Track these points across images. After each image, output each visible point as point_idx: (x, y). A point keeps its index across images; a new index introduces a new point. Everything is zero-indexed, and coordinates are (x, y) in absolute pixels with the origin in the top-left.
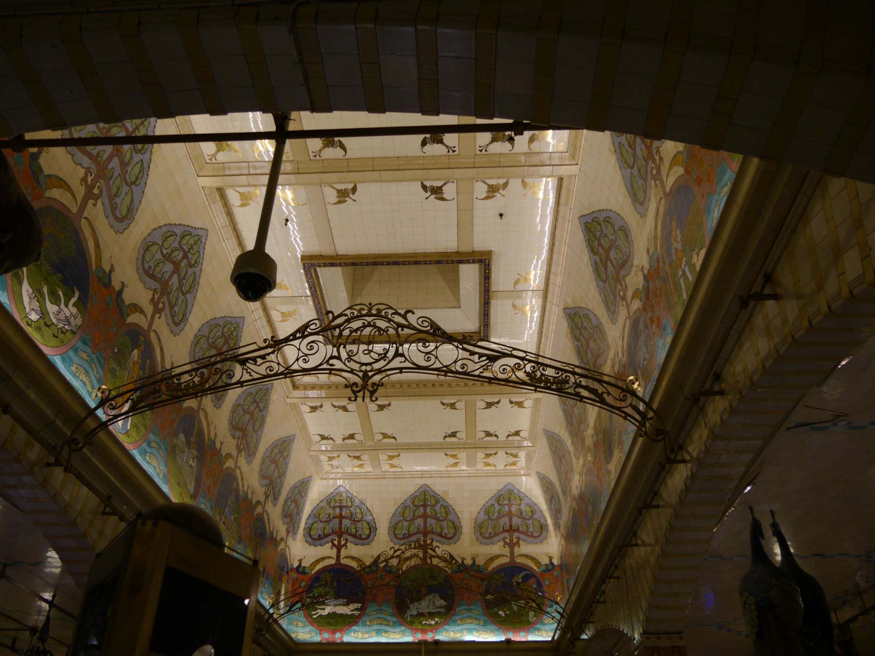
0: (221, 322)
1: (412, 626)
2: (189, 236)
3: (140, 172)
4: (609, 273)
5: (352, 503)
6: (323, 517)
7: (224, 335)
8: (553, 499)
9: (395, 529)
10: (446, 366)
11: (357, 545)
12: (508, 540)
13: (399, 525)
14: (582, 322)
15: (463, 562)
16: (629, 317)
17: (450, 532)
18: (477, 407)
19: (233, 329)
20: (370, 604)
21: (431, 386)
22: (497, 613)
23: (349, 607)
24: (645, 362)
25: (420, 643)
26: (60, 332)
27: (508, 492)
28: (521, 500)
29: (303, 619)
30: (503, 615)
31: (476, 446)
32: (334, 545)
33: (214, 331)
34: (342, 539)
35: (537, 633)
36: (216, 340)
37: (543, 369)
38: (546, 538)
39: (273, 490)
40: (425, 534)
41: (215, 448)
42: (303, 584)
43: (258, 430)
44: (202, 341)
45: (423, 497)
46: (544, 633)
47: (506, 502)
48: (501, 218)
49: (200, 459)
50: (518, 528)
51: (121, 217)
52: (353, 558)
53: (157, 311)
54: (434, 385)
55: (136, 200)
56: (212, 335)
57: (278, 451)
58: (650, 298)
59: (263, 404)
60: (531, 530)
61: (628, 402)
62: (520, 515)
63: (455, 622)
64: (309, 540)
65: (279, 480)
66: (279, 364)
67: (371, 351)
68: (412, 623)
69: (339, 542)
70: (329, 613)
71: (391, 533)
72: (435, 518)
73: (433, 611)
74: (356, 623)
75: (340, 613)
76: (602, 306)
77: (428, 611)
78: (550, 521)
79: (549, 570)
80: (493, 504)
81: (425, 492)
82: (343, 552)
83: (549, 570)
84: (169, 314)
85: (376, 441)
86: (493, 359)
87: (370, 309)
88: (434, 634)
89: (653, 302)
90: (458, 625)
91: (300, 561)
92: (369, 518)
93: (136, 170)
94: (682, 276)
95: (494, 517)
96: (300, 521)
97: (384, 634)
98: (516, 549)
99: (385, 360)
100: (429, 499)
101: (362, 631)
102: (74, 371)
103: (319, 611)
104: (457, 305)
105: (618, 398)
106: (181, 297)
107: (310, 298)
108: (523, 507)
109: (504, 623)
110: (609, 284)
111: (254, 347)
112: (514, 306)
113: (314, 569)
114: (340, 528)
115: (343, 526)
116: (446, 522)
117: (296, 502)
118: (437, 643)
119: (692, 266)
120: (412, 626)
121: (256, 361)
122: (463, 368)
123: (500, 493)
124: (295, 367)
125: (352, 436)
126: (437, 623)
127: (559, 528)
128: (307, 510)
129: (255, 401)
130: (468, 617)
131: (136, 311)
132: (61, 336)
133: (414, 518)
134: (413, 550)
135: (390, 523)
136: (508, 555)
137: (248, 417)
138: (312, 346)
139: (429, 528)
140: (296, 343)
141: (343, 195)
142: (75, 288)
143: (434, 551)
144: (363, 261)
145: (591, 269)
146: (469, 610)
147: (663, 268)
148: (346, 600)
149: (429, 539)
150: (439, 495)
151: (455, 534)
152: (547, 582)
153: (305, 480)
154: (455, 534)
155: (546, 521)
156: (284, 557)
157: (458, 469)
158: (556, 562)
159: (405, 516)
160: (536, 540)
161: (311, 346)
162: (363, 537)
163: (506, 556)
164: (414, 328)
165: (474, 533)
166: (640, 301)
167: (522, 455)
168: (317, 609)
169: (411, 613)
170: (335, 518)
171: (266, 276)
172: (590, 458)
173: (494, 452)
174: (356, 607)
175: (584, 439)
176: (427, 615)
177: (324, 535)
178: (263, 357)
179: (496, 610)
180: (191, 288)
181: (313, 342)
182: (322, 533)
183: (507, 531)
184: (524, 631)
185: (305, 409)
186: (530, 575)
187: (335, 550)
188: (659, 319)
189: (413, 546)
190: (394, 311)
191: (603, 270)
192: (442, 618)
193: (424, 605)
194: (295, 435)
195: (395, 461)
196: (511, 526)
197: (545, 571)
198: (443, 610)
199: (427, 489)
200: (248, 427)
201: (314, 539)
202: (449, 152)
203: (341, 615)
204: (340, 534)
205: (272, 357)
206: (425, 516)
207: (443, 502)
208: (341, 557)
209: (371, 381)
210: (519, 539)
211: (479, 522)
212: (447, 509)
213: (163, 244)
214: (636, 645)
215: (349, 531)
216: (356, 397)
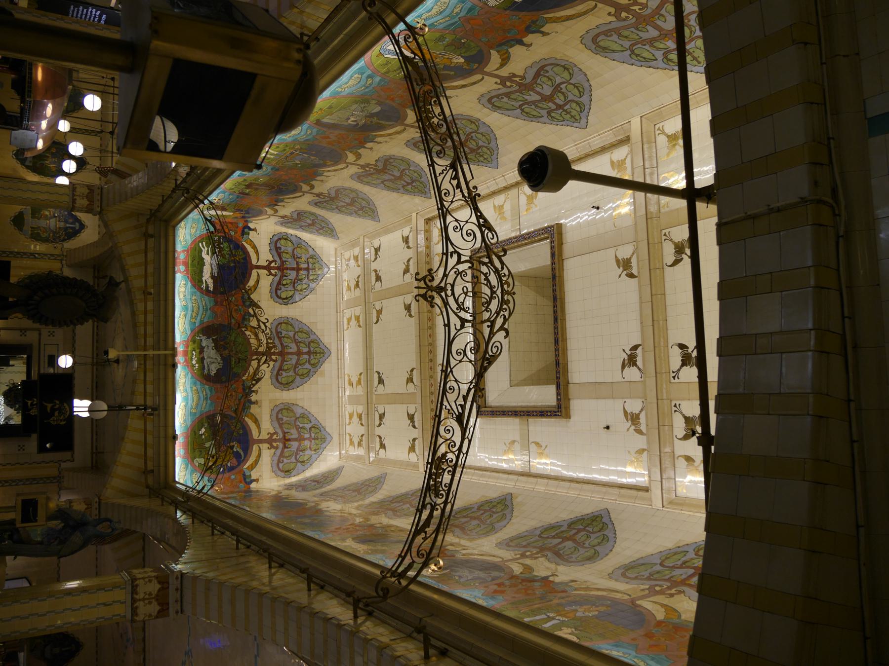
0: (493, 144)
2: (579, 110)
3: (645, 58)
4: (549, 540)
6: (298, 252)
7: (479, 148)
9: (286, 323)
10: (451, 371)
12: (275, 437)
14: (499, 512)
15: (254, 391)
16: (504, 561)
19: (485, 157)
20: (213, 299)
22: (202, 426)
24: (457, 578)
25: (174, 349)
27: (323, 437)
28: (315, 450)
29: (198, 233)
32: (271, 262)
33: (484, 138)
35: (183, 466)
36: (474, 140)
37: (449, 471)
38: (277, 476)
39: (324, 202)
40: (282, 354)
41: (366, 142)
42: (233, 233)
43: (385, 185)
44: (473, 126)
45: (318, 351)
46: (183, 474)
47: (313, 435)
48: (605, 428)
49: (356, 128)
50: (288, 448)
51: (597, 41)
52: (258, 282)
53: (503, 81)
54: (431, 360)
55: (616, 55)
56: (479, 136)
58: (524, 584)
59: (410, 189)
60: (285, 461)
61: (417, 559)
62: (300, 450)
63: (195, 384)
64: (276, 238)
65: (335, 207)
66: (452, 202)
67: (466, 295)
68: (194, 341)
69: (274, 268)
72: (297, 362)
73: (205, 362)
74: (194, 285)
76: (514, 534)
78: (294, 479)
79: (245, 479)
80: (311, 422)
83: (245, 479)
84: (500, 92)
86: (459, 419)
87: (509, 293)
89: (520, 586)
90: (191, 388)
91: (255, 230)
92: (297, 297)
93: (646, 54)
94: (548, 616)
95: (298, 423)
97: (183, 313)
98: (266, 445)
99: (457, 309)
103: (206, 249)
104: (513, 383)
105: (420, 549)
106: (517, 104)
107: (518, 233)
108: (308, 452)
109: (193, 432)
110: (538, 541)
111: (469, 177)
112: (514, 442)
114: (287, 269)
115: (289, 271)
117: (313, 224)
118: (174, 366)
119: (559, 627)
121: (454, 179)
122: (450, 388)
123: (322, 429)
124: (449, 219)
125: (378, 279)
126: (193, 366)
127: (288, 489)
128: (305, 236)
129: (413, 182)
130: (199, 398)
131: (503, 60)
133: (297, 343)
134: (265, 342)
135: (293, 319)
136: (260, 438)
137: (397, 174)
138: (471, 235)
139: (287, 357)
140: (474, 219)
141: (625, 264)
143: (265, 363)
144: (557, 286)
145: (552, 522)
146: (206, 399)
147: (555, 597)
148: (216, 275)
149: (276, 358)
151: (281, 383)
152: (233, 477)
154: (281, 383)
155: (294, 476)
156: (259, 213)
158: (253, 486)
159: (300, 334)
160: (275, 468)
161: (470, 234)
162: (279, 292)
163: (259, 435)
164: (490, 338)
166: (521, 573)
167: (361, 452)
168: (208, 247)
169: (203, 340)
170: (297, 263)
171: (545, 182)
172: (358, 520)
173: (363, 422)
176: (201, 356)
178: (459, 186)
179: (206, 425)
180: (527, 113)
181: (475, 236)
182: (282, 250)
183: (284, 436)
184: (185, 454)
185: (406, 232)
186: (240, 459)
187: (266, 264)
188: (503, 592)
189: (269, 341)
190: (507, 317)
191: (553, 534)
192: (198, 371)
193: (211, 353)
195: (354, 322)
196: (289, 440)
197: (244, 475)
198: (206, 372)
199: (326, 356)
201: (276, 244)
202: (673, 372)
203: (202, 271)
204: (281, 268)
205: (459, 196)
206: (299, 353)
208: (259, 271)
209: (434, 294)
210: (277, 448)
211: (294, 408)
212: (306, 375)
213: (571, 84)
214: (171, 566)
215: (284, 278)
216: (420, 280)
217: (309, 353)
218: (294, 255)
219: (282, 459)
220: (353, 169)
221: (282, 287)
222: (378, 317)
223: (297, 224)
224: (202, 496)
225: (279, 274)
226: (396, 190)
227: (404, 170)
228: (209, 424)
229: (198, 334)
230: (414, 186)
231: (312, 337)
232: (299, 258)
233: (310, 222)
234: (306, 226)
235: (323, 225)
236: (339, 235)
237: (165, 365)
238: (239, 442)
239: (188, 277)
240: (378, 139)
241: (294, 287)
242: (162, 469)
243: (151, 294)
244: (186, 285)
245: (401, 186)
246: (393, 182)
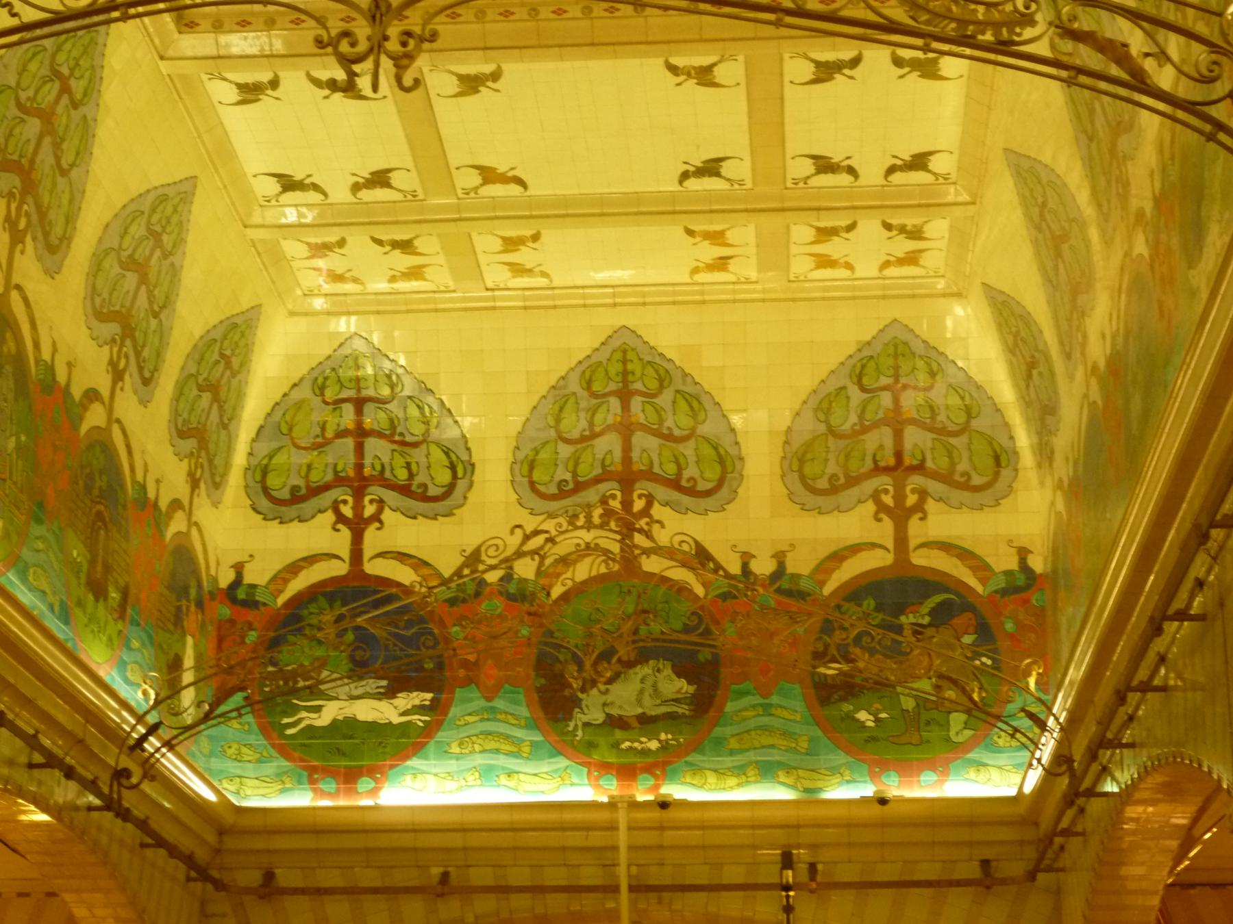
1: (589, 756)
6: (304, 433)
8: (1035, 372)
9: (531, 467)
11: (415, 518)
12: (888, 500)
13: (544, 455)
17: (708, 475)
18: (787, 79)
22: (850, 718)
23: (395, 702)
27: (891, 350)
28: (933, 374)
29: (258, 740)
30: (871, 724)
31: (788, 204)
32: (341, 518)
34: (367, 499)
39: (138, 354)
40: (627, 479)
42: (252, 636)
43: (72, 165)
45: (620, 367)
47: (884, 381)
50: (923, 461)
52: (402, 557)
57: (143, 232)
59: (83, 83)
60: (963, 466)
63: (719, 742)
64: (264, 503)
65: (154, 323)
68: (591, 745)
69: (358, 507)
70: (335, 721)
71: (518, 478)
72: (657, 434)
74: (416, 748)
75: (370, 719)
77: (640, 711)
78: (1023, 440)
80: (844, 388)
81: (625, 352)
82: (373, 540)
83: (1017, 590)
85: (460, 192)
88: (656, 777)
90: (732, 753)
91: (239, 568)
95: (847, 427)
96: (230, 448)
97: (503, 779)
98: (914, 525)
100: (638, 373)
101: (434, 771)
103: (304, 714)
108: (939, 394)
113: (281, 592)
114: (359, 467)
115: (367, 461)
116: (691, 444)
117: (213, 388)
120: (589, 756)
123: (866, 353)
125: (380, 179)
126: (665, 746)
127: (1051, 459)
129: (57, 74)
135: (517, 448)
136: (890, 545)
137: (33, 126)
139: (639, 465)
143: (648, 535)
146: (767, 709)
148: (384, 683)
149: (640, 496)
150: (670, 360)
151: (721, 483)
152: (1009, 626)
153: (238, 320)
154: (721, 483)
155: (1012, 438)
156: (183, 554)
157: (732, 278)
158: (1037, 564)
159: (564, 426)
162: (433, 491)
165: (783, 477)
167: (938, 228)
168: (297, 709)
169: (585, 719)
172: (1141, 247)
174: (417, 702)
175: (1126, 185)
176: (635, 724)
177: (308, 487)
179: (847, 707)
183: (887, 470)
184: (934, 770)
185: (222, 92)
187: (345, 533)
192: (681, 733)
194: (196, 177)
195: (524, 256)
196: (899, 455)
197: (1004, 592)
199: (632, 342)
200: (38, 161)
207: (684, 382)
210: (923, 494)
211: (797, 443)
212: (695, 404)
215: (388, 474)
217: (625, 395)
218: (316, 447)
219: (957, 478)
222: (504, 179)
223: (214, 437)
224: (1057, 719)
225: (375, 491)
226: (87, 130)
227: (20, 106)
228: (843, 699)
229: (564, 734)
230: (72, 70)
231: (574, 386)
232: (323, 429)
233: (207, 397)
234: (221, 408)
235: (216, 356)
236: (245, 306)
237: (662, 828)
238: (900, 609)
239: (392, 767)
241: (415, 445)
242: (979, 835)
243: (445, 876)
244: (416, 773)
245: (73, 112)
246: (63, 140)
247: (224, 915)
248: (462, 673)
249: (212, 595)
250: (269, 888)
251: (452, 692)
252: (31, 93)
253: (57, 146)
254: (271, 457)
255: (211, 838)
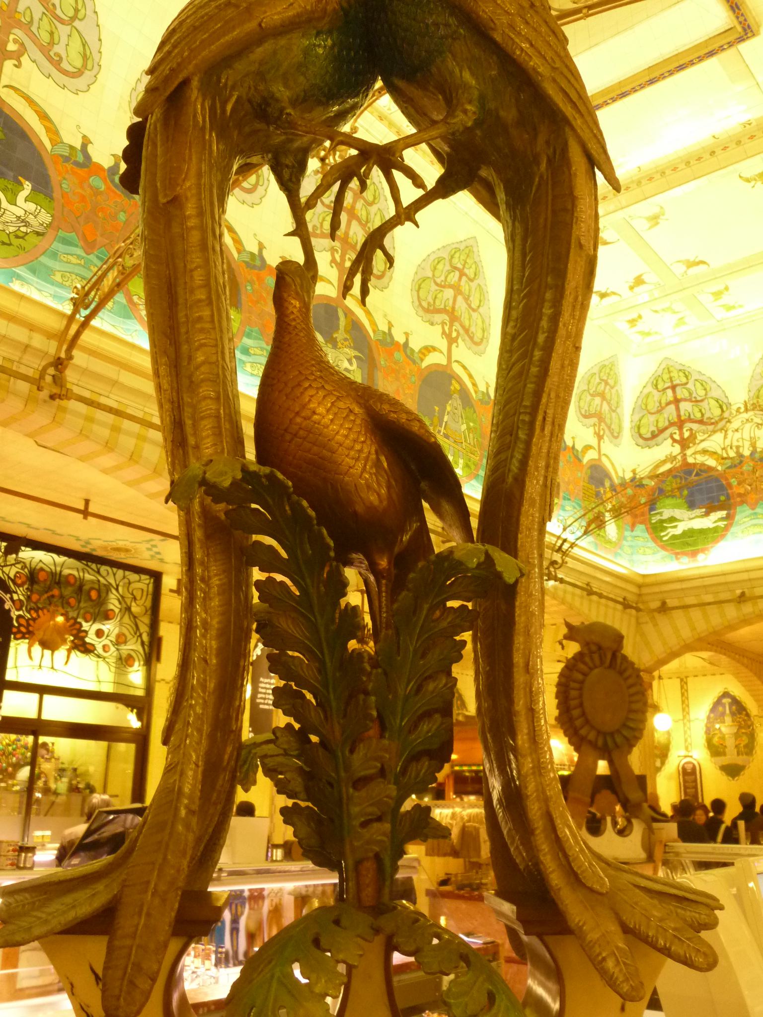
5: (686, 377)
6: (653, 406)
21: (708, 156)
26: (12, 237)
29: (652, 544)
32: (675, 441)
34: (684, 430)
51: (75, 70)
55: (91, 39)
64: (641, 441)
69: (681, 434)
74: (723, 536)
91: (634, 471)
92: (715, 393)
102: (60, 280)
103: (670, 530)
114: (679, 416)
115: (682, 413)
125: (639, 281)
132: (16, 242)
137: (449, 293)
142: (20, 178)
168: (666, 528)
170: (668, 404)
182: (655, 429)
200: (457, 307)
203: (702, 531)
215: (692, 417)
220: (461, 352)
221: (706, 416)
232: (660, 403)
234: (609, 403)
235: (598, 380)
240: (384, 327)
241: (702, 401)
243: (743, 594)
245: (471, 284)
246: (469, 296)
247: (647, 623)
248: (738, 499)
249: (621, 485)
250: (664, 608)
251: (735, 509)
252: (443, 278)
253: (467, 299)
254: (640, 421)
255: (634, 589)
